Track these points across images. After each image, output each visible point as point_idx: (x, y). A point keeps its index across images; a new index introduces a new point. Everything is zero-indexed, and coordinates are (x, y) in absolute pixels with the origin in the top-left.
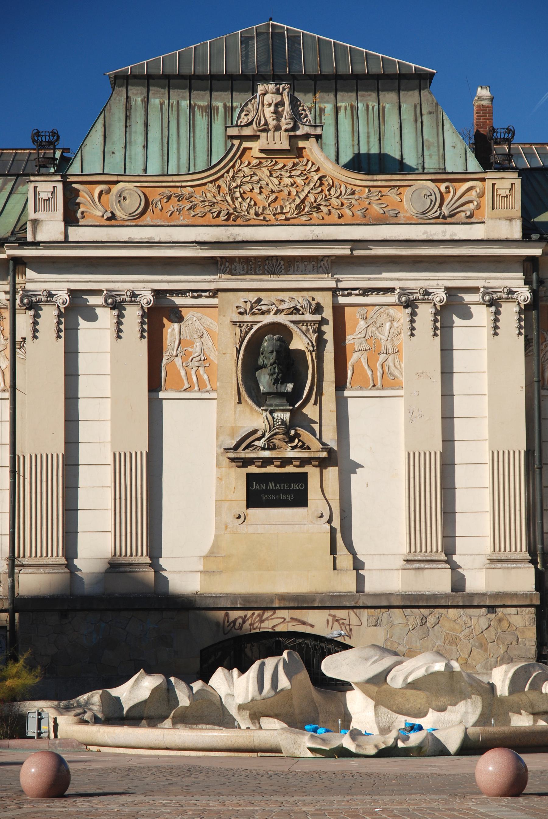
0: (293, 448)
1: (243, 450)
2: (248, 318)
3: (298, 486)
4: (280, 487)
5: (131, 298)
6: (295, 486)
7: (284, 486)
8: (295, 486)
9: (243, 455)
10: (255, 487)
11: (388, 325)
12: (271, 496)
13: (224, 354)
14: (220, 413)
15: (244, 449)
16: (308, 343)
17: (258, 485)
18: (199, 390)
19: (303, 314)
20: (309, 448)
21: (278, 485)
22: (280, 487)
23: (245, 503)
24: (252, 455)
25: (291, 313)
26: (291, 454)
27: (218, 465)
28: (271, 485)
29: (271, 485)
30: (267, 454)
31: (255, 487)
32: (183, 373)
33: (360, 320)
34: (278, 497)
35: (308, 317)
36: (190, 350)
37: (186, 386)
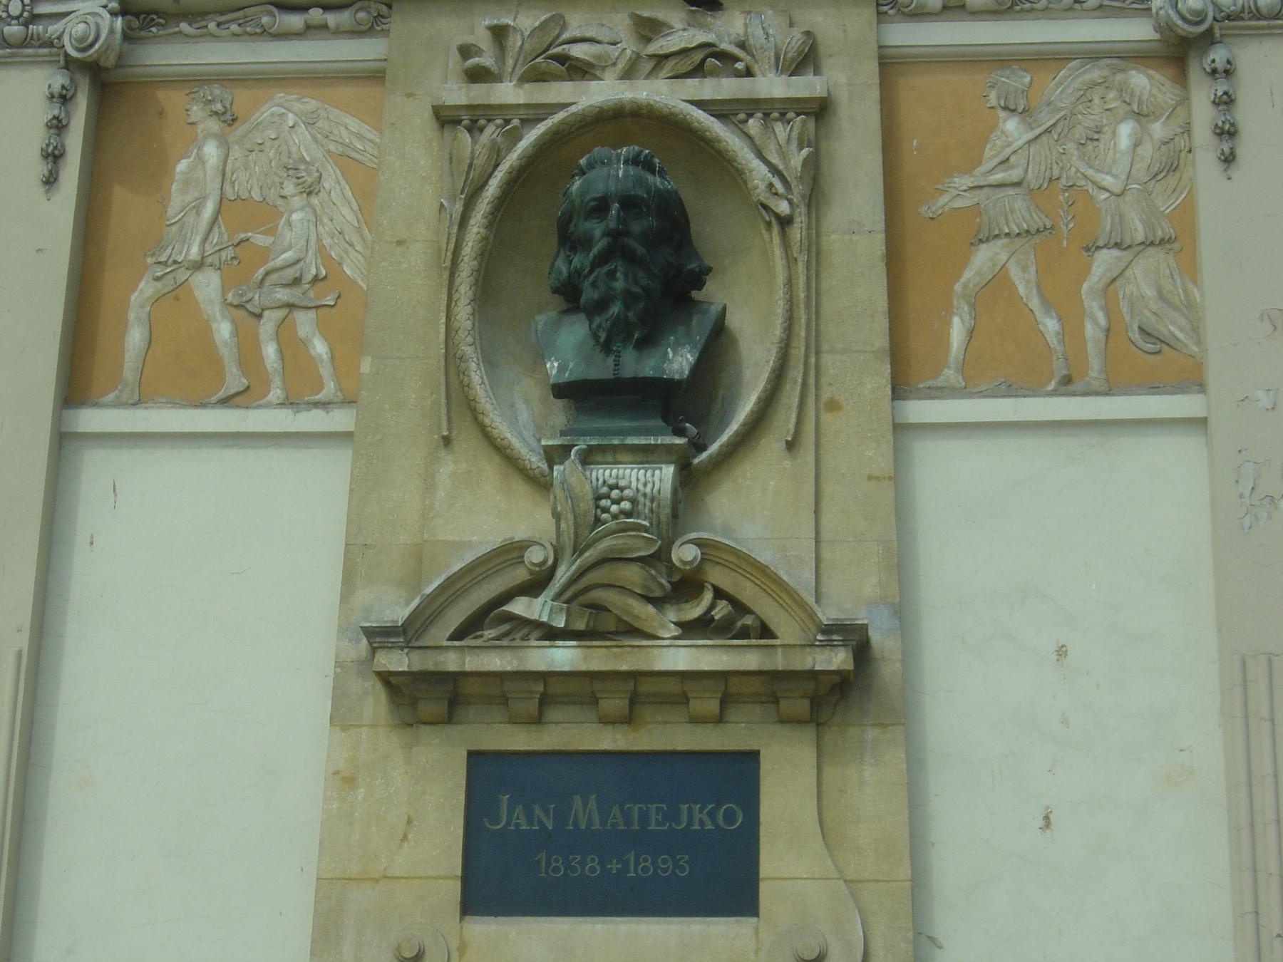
0: (690, 629)
1: (453, 637)
2: (508, 93)
3: (712, 815)
4: (628, 820)
5: (26, 25)
6: (696, 816)
7: (644, 818)
8: (696, 816)
9: (451, 662)
10: (509, 815)
11: (1126, 130)
12: (583, 863)
13: (400, 243)
14: (364, 488)
15: (459, 634)
16: (771, 185)
17: (519, 809)
18: (290, 402)
19: (749, 73)
20: (765, 631)
21: (616, 810)
22: (628, 820)
23: (454, 889)
24: (496, 662)
25: (698, 71)
26: (679, 657)
27: (341, 718)
28: (585, 812)
29: (585, 812)
30: (563, 657)
31: (509, 815)
32: (223, 330)
33: (1002, 114)
34: (614, 866)
35: (771, 85)
36: (261, 240)
37: (234, 381)
